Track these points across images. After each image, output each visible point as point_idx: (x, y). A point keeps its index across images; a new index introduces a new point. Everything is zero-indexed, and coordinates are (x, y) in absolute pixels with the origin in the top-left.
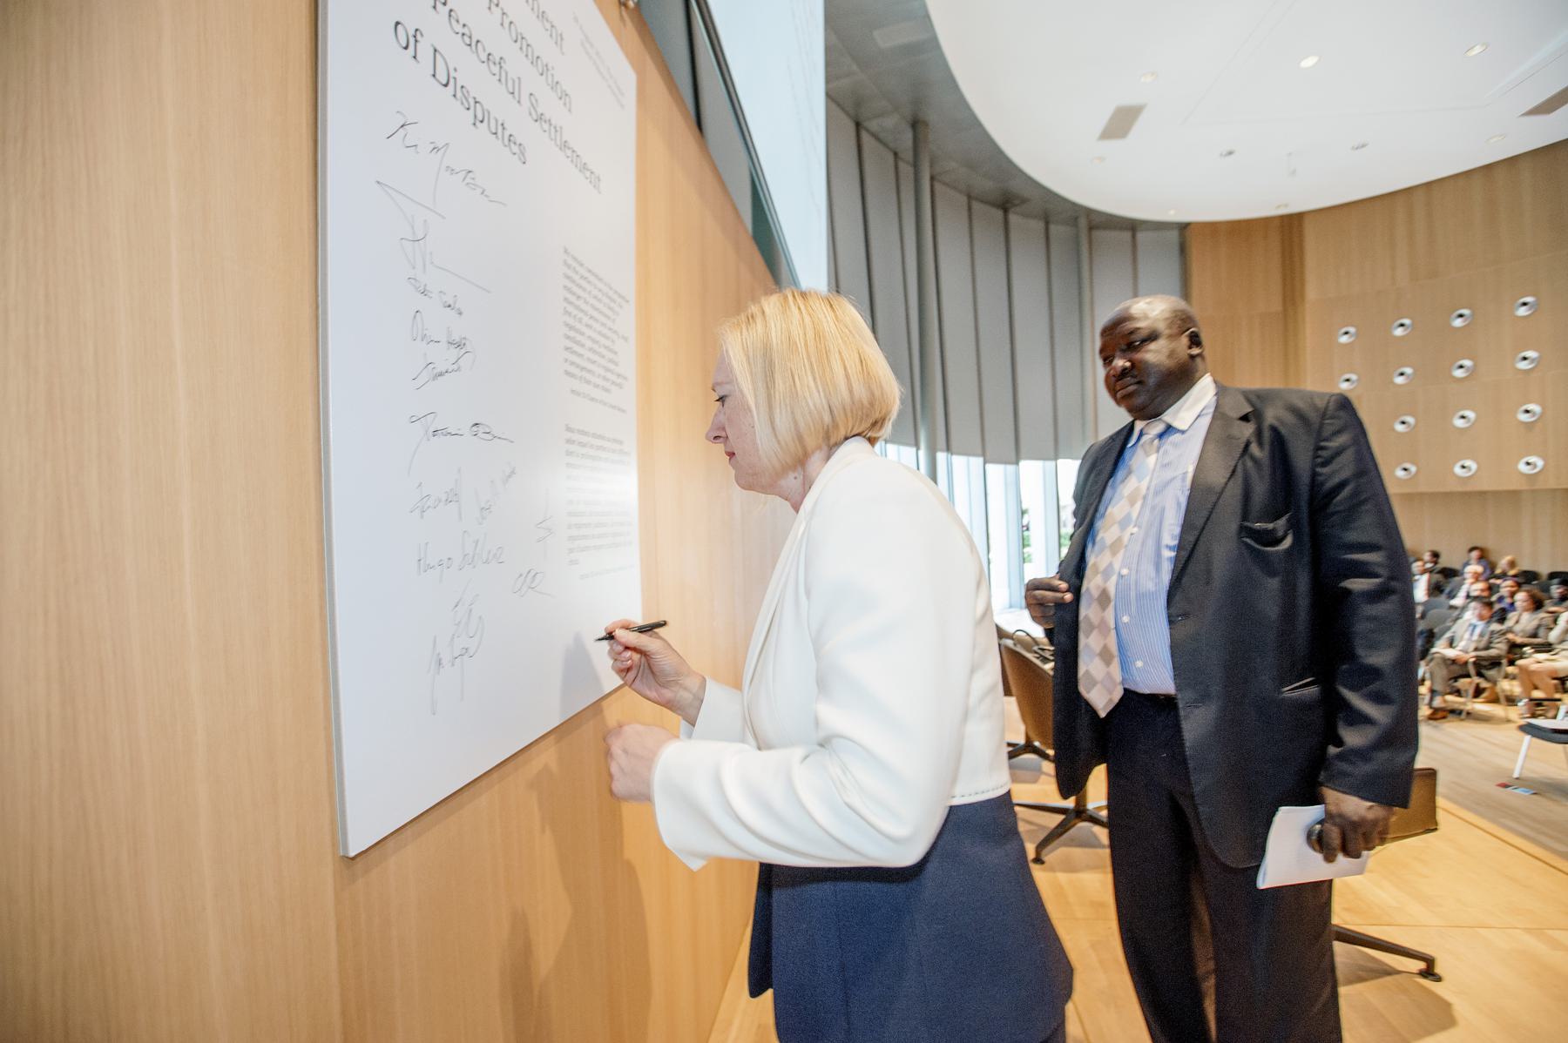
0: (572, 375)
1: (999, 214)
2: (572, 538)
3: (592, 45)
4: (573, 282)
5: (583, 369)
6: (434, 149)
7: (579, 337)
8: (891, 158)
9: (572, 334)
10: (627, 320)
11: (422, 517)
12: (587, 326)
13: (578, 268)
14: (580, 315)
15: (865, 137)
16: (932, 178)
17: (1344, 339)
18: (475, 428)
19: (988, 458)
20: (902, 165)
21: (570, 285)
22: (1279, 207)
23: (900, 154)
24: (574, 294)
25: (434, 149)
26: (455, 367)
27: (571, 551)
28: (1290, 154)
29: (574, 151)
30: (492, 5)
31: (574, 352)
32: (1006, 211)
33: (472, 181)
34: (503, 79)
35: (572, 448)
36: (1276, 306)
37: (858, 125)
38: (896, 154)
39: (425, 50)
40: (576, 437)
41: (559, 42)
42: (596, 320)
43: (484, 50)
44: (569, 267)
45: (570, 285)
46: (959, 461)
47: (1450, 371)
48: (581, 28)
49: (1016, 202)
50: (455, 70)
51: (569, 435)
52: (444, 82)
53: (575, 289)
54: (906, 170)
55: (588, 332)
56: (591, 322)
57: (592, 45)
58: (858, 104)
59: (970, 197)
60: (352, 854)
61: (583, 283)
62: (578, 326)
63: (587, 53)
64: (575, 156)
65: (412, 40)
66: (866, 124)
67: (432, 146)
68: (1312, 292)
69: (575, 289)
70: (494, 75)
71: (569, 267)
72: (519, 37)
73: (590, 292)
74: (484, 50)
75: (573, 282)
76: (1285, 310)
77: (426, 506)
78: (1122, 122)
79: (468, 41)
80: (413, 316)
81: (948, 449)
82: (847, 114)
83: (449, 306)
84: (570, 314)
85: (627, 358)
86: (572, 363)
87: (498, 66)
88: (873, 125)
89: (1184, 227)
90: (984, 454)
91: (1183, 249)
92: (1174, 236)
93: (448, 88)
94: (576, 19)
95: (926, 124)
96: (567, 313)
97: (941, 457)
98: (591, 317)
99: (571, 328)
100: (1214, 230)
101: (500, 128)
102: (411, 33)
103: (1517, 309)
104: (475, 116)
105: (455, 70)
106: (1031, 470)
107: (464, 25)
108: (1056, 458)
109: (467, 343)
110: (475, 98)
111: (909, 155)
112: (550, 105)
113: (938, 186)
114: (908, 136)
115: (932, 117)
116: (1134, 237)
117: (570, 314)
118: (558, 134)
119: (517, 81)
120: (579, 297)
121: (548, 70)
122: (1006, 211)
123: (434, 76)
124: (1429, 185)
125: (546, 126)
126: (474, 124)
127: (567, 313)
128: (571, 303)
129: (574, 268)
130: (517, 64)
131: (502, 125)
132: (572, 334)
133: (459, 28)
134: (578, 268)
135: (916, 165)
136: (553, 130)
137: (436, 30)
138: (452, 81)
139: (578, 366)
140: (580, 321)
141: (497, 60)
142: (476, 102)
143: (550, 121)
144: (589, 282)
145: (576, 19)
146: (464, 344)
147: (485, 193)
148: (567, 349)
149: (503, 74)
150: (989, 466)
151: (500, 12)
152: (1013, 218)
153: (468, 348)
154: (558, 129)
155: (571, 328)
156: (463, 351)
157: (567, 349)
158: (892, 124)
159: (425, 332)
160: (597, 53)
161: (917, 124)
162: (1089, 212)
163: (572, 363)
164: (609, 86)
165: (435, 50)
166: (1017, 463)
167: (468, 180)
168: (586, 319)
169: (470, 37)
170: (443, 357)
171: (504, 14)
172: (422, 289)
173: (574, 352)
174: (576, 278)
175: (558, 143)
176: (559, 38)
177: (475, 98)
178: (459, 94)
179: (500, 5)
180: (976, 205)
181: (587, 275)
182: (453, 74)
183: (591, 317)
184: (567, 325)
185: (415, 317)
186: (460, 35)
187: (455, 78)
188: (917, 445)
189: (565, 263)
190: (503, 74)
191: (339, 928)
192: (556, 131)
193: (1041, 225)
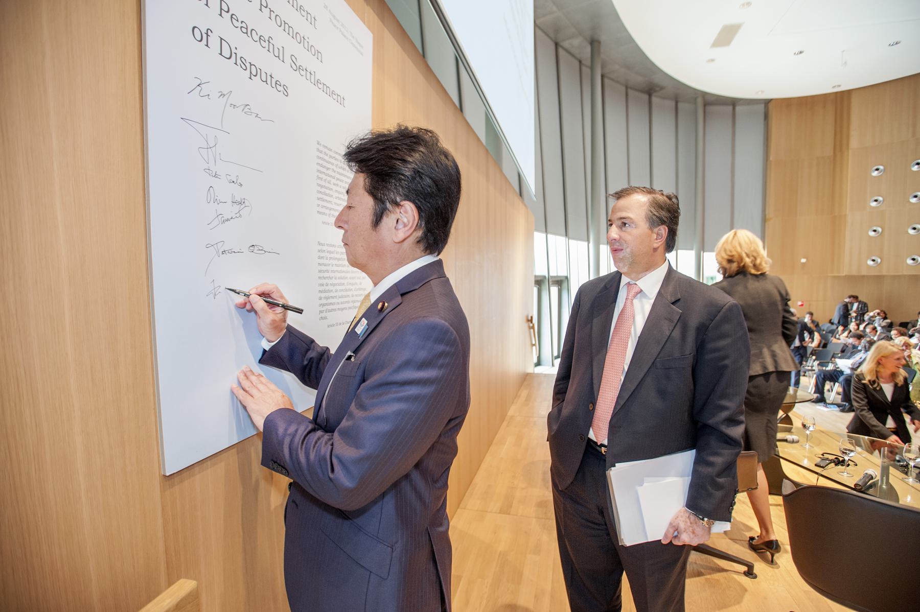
0: (324, 214)
1: (646, 97)
2: (323, 305)
3: (338, 21)
4: (324, 160)
5: (331, 209)
6: (221, 95)
7: (328, 191)
8: (578, 63)
9: (323, 190)
11: (215, 298)
12: (334, 184)
13: (328, 152)
14: (329, 179)
15: (561, 51)
16: (603, 76)
17: (875, 174)
18: (251, 248)
20: (584, 68)
21: (321, 162)
23: (583, 62)
24: (324, 167)
25: (221, 95)
26: (238, 215)
27: (321, 312)
28: (843, 51)
29: (324, 84)
30: (262, 7)
31: (324, 200)
32: (650, 95)
33: (249, 111)
34: (271, 50)
35: (322, 255)
36: (829, 151)
37: (557, 45)
38: (580, 62)
39: (214, 40)
40: (324, 248)
41: (313, 23)
42: (341, 181)
43: (257, 35)
44: (321, 152)
45: (321, 162)
47: (909, 199)
48: (330, 11)
49: (657, 89)
50: (236, 48)
51: (320, 247)
52: (228, 57)
53: (325, 164)
54: (586, 71)
55: (334, 188)
56: (338, 182)
57: (338, 21)
58: (557, 30)
59: (627, 88)
60: (168, 474)
61: (332, 161)
62: (327, 185)
63: (335, 26)
64: (325, 88)
65: (205, 36)
66: (562, 44)
67: (220, 93)
68: (854, 142)
69: (325, 164)
70: (264, 48)
71: (321, 152)
72: (283, 23)
73: (337, 165)
74: (257, 35)
75: (324, 160)
77: (217, 293)
78: (727, 36)
79: (244, 30)
80: (208, 189)
82: (550, 38)
83: (234, 182)
84: (321, 179)
86: (323, 207)
87: (267, 42)
88: (566, 44)
89: (767, 102)
91: (766, 116)
93: (230, 60)
94: (326, 7)
95: (599, 42)
96: (318, 178)
98: (338, 179)
99: (322, 186)
100: (787, 103)
101: (269, 78)
102: (204, 31)
103: (913, 166)
104: (251, 72)
105: (236, 48)
107: (242, 22)
109: (246, 201)
110: (250, 63)
111: (588, 63)
112: (306, 59)
113: (606, 80)
114: (588, 49)
115: (603, 38)
116: (734, 109)
117: (321, 179)
118: (313, 77)
119: (281, 49)
120: (328, 169)
121: (304, 39)
123: (221, 54)
125: (303, 73)
126: (250, 78)
127: (318, 178)
128: (321, 172)
129: (325, 153)
130: (281, 39)
131: (271, 76)
132: (323, 190)
133: (239, 24)
134: (328, 152)
135: (592, 68)
136: (308, 74)
137: (222, 27)
138: (234, 55)
139: (327, 208)
140: (329, 182)
141: (267, 39)
142: (251, 65)
143: (306, 69)
144: (336, 159)
145: (326, 7)
146: (244, 202)
147: (258, 116)
148: (318, 199)
149: (271, 46)
151: (269, 10)
152: (655, 100)
153: (247, 203)
154: (313, 73)
155: (322, 186)
156: (244, 205)
157: (318, 199)
158: (577, 44)
159: (216, 197)
160: (342, 25)
161: (594, 43)
162: (704, 94)
163: (323, 207)
164: (352, 43)
165: (221, 39)
167: (246, 110)
168: (333, 181)
169: (247, 29)
170: (229, 210)
171: (271, 11)
172: (214, 175)
173: (324, 200)
174: (327, 158)
175: (313, 81)
176: (313, 19)
177: (250, 63)
178: (239, 62)
179: (269, 7)
180: (630, 92)
181: (334, 155)
182: (234, 51)
183: (338, 179)
184: (319, 185)
185: (209, 190)
186: (239, 28)
187: (236, 54)
189: (318, 149)
190: (271, 46)
191: (163, 509)
192: (310, 73)
193: (673, 103)
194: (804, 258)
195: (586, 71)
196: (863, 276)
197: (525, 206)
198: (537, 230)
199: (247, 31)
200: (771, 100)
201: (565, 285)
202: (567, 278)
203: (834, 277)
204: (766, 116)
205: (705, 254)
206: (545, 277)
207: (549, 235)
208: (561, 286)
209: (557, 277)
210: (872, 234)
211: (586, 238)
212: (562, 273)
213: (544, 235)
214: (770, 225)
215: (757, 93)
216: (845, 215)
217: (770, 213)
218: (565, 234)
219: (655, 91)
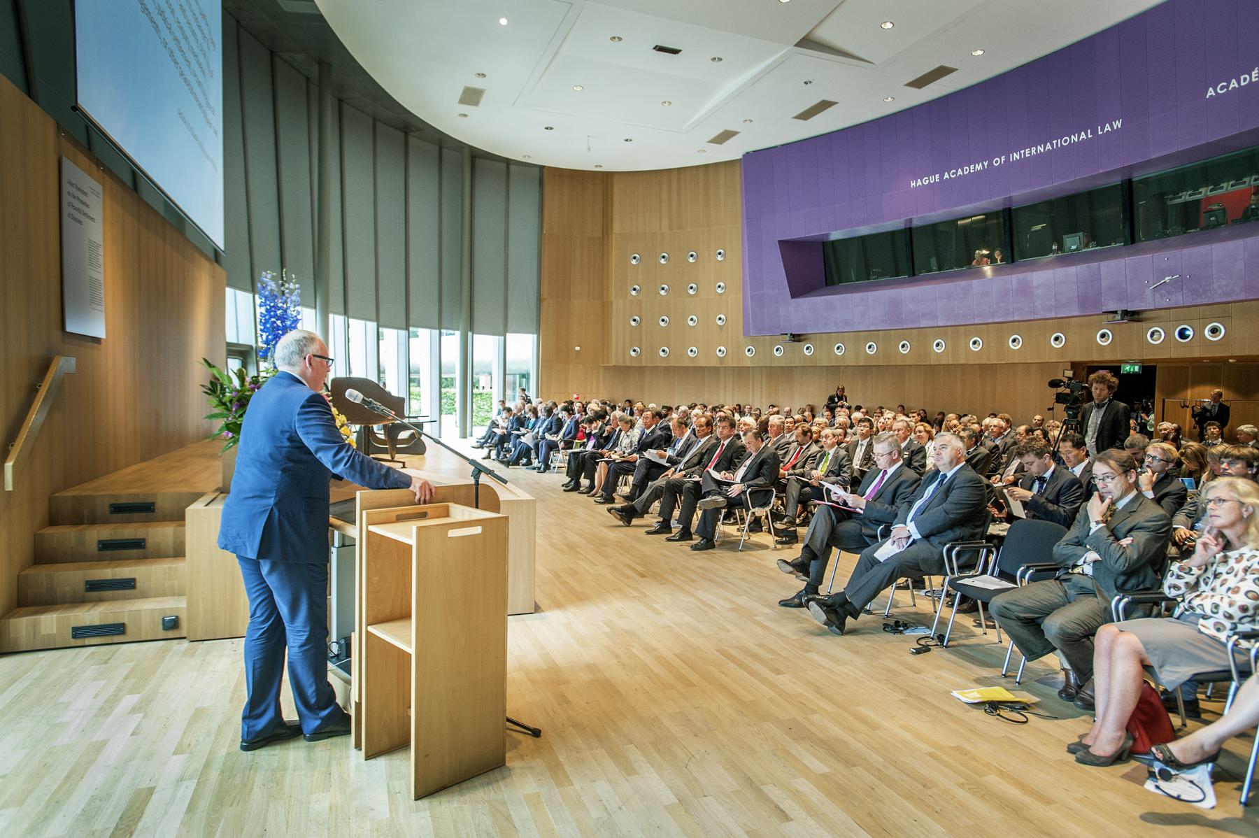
1: (402, 135)
15: (278, 61)
17: (634, 262)
19: (381, 322)
22: (596, 166)
28: (588, 136)
32: (406, 134)
36: (598, 234)
37: (272, 53)
38: (308, 79)
46: (357, 325)
49: (414, 129)
54: (314, 89)
59: (374, 119)
68: (616, 228)
76: (603, 236)
78: (471, 96)
81: (346, 313)
89: (542, 168)
90: (377, 320)
91: (541, 183)
106: (424, 337)
108: (440, 328)
113: (346, 108)
114: (316, 68)
116: (508, 168)
122: (406, 134)
150: (384, 331)
152: (412, 140)
162: (471, 147)
166: (407, 328)
180: (379, 124)
188: (315, 308)
193: (437, 149)
194: (578, 346)
195: (314, 89)
196: (629, 368)
200: (544, 166)
203: (606, 368)
204: (541, 183)
205: (475, 336)
210: (633, 323)
211: (314, 305)
213: (251, 295)
214: (544, 305)
216: (611, 302)
217: (545, 295)
219: (412, 131)
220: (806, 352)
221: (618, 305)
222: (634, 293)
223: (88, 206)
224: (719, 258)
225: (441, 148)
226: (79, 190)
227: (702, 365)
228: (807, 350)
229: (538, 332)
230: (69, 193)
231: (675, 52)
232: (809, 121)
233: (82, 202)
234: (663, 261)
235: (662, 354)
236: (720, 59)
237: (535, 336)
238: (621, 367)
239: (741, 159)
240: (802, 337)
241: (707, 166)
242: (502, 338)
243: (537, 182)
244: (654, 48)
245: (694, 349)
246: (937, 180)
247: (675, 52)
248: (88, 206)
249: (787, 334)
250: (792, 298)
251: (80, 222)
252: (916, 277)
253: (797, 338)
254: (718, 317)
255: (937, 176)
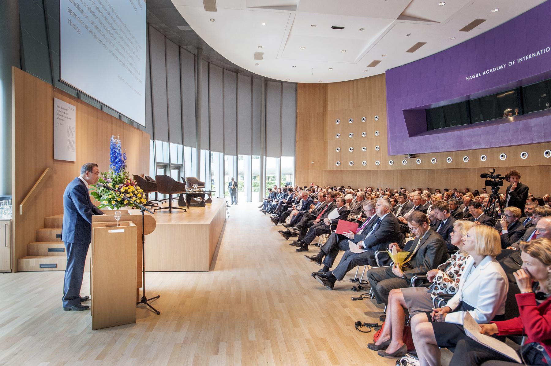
1: (235, 74)
8: (193, 56)
10: (74, 130)
17: (337, 123)
28: (312, 68)
32: (237, 73)
36: (321, 111)
38: (195, 55)
59: (223, 69)
68: (329, 108)
78: (259, 56)
85: (74, 133)
89: (297, 84)
90: (224, 152)
91: (296, 90)
92: (295, 85)
97: (204, 153)
100: (304, 85)
106: (244, 159)
108: (251, 155)
112: (66, 115)
113: (211, 65)
116: (282, 84)
122: (237, 73)
124: (357, 80)
150: (226, 157)
152: (240, 76)
162: (264, 77)
166: (237, 155)
180: (225, 71)
193: (251, 78)
197: (140, 130)
198: (151, 139)
199: (61, 116)
201: (181, 169)
202: (182, 165)
203: (325, 171)
204: (296, 90)
206: (168, 164)
207: (171, 144)
208: (179, 170)
209: (178, 164)
210: (337, 151)
212: (180, 163)
215: (287, 79)
217: (298, 139)
218: (182, 143)
219: (239, 72)
220: (403, 164)
221: (330, 142)
222: (337, 137)
223: (67, 114)
224: (376, 119)
225: (252, 78)
226: (62, 108)
227: (369, 169)
228: (418, 162)
229: (295, 155)
230: (57, 110)
231: (342, 28)
232: (414, 52)
233: (64, 113)
234: (350, 122)
235: (350, 164)
236: (363, 29)
237: (294, 157)
238: (332, 171)
239: (385, 73)
240: (416, 156)
241: (370, 77)
242: (279, 158)
243: (295, 90)
244: (332, 28)
245: (365, 162)
246: (479, 76)
247: (342, 28)
248: (67, 114)
249: (408, 154)
250: (410, 137)
251: (63, 120)
252: (471, 125)
253: (413, 156)
254: (350, 148)
255: (479, 74)
